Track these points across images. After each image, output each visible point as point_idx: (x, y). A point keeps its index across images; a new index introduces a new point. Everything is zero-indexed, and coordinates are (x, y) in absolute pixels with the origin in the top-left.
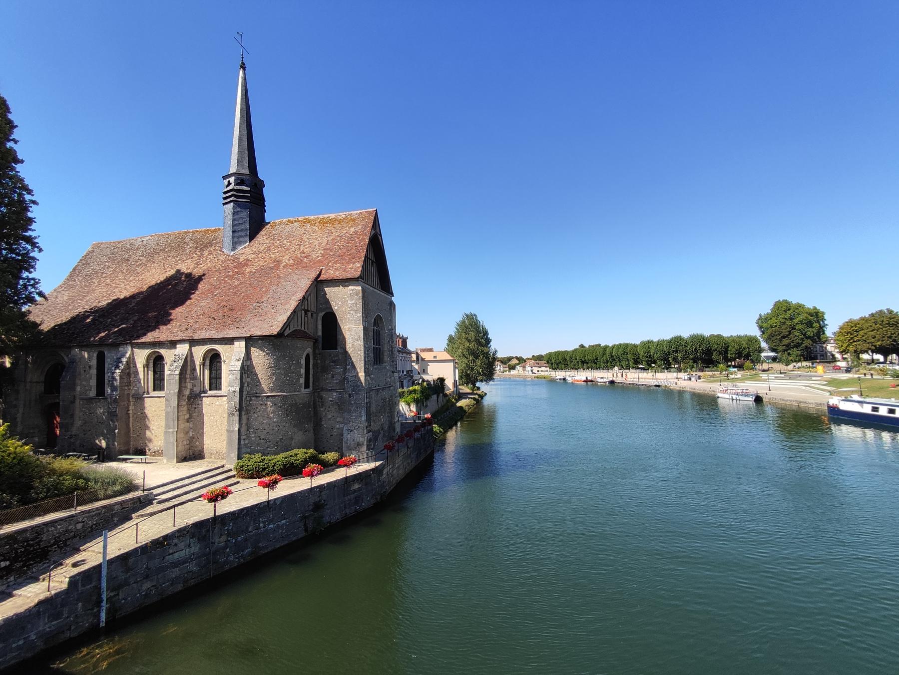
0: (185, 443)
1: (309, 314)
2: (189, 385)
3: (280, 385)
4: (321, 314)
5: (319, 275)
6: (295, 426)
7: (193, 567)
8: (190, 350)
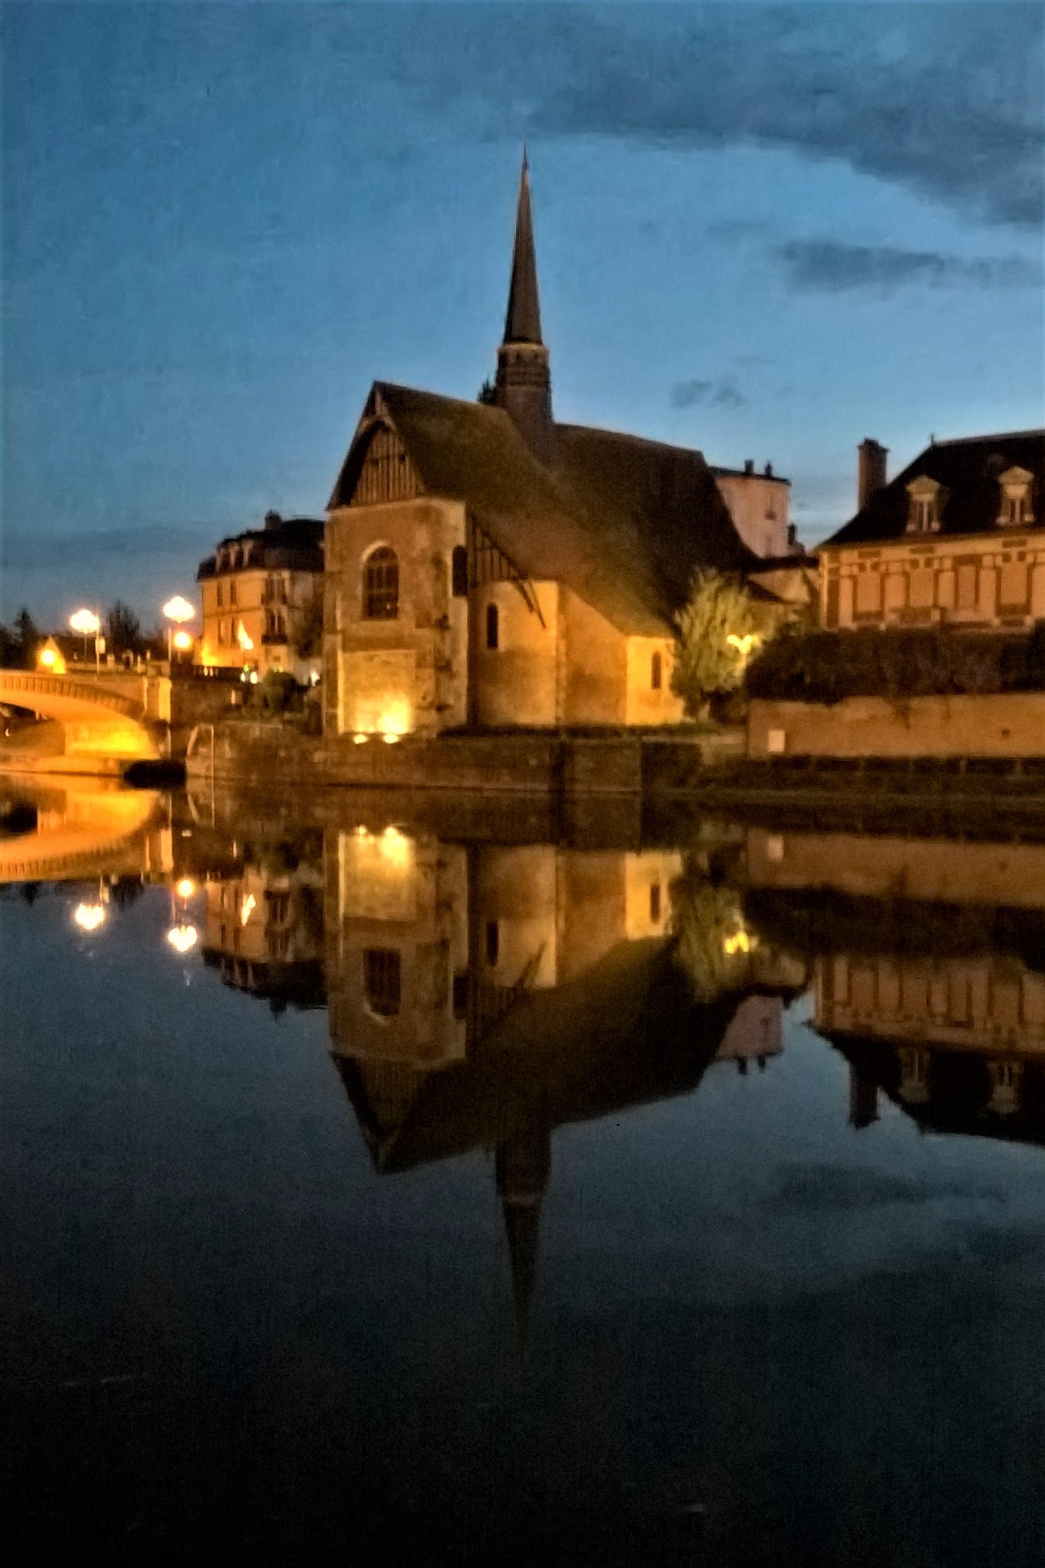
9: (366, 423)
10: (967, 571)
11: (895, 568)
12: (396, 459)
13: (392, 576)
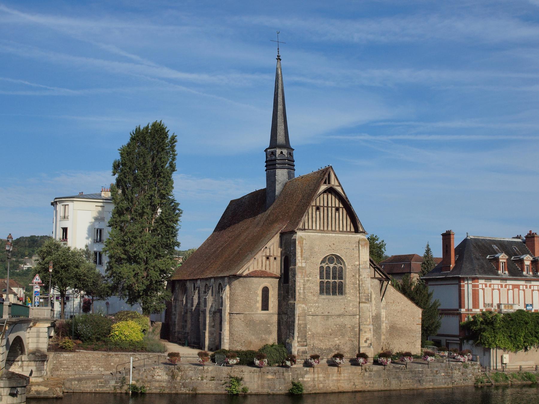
1: (272, 259)
7: (164, 384)
10: (516, 290)
11: (496, 287)
12: (334, 209)
13: (339, 274)
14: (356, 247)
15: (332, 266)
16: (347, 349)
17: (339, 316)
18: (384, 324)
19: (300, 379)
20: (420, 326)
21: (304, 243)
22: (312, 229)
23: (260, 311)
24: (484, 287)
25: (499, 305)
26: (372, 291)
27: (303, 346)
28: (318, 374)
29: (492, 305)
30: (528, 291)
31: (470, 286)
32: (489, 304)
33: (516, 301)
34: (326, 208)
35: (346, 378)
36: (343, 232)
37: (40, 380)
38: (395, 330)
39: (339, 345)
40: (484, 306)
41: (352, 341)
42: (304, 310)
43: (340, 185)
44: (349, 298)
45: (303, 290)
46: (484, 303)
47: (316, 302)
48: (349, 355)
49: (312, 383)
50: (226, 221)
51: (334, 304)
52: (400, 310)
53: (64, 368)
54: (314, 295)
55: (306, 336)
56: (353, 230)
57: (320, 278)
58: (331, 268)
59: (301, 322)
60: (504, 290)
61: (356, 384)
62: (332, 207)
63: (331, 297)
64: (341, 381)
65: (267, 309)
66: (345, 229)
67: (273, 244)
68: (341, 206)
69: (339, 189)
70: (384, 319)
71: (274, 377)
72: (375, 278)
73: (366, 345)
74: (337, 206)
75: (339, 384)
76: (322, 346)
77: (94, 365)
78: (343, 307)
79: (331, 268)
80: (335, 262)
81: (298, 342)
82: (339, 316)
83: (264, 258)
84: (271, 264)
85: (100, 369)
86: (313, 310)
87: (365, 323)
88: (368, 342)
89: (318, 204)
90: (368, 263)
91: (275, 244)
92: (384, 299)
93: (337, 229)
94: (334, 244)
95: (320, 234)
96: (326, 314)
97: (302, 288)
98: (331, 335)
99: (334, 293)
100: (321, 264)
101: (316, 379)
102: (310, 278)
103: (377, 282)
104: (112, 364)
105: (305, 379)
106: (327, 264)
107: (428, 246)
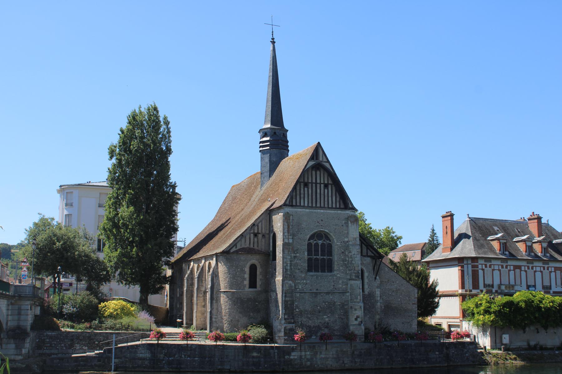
0: (202, 320)
2: (204, 285)
3: (231, 286)
4: (272, 235)
5: (272, 205)
6: (240, 313)
8: (205, 263)
9: (311, 163)
10: (518, 271)
11: (496, 267)
12: (322, 185)
13: (328, 250)
14: (345, 223)
15: (320, 242)
16: (337, 328)
17: (328, 293)
18: (379, 304)
19: (286, 357)
20: (416, 306)
21: (291, 219)
22: (300, 206)
23: (247, 289)
24: (484, 267)
25: (499, 286)
26: (364, 269)
27: (290, 323)
28: (305, 352)
29: (492, 286)
30: (530, 272)
31: (470, 266)
32: (489, 285)
33: (518, 282)
34: (314, 185)
35: (335, 356)
36: (332, 208)
37: (20, 357)
38: (389, 309)
39: (328, 323)
40: (484, 287)
41: (342, 319)
42: (290, 286)
43: (328, 161)
44: (338, 275)
45: (290, 266)
46: (484, 284)
47: (305, 279)
48: (339, 334)
49: (299, 361)
50: (226, 206)
51: (323, 282)
52: (395, 290)
53: (47, 347)
54: (302, 272)
55: (293, 313)
56: (342, 206)
57: (308, 255)
58: (320, 244)
59: (287, 299)
60: (504, 270)
61: (345, 362)
62: (320, 184)
63: (320, 274)
64: (329, 360)
65: (255, 287)
66: (334, 206)
67: (261, 221)
68: (330, 182)
69: (327, 165)
70: (379, 299)
71: (259, 355)
72: (368, 256)
73: (357, 322)
74: (326, 182)
75: (327, 362)
76: (310, 323)
77: (77, 344)
78: (333, 284)
79: (320, 244)
80: (324, 238)
81: (285, 319)
82: (328, 293)
83: (252, 235)
84: (260, 241)
85: (84, 347)
86: (300, 287)
87: (355, 300)
88: (359, 320)
89: (306, 180)
90: (358, 239)
91: (263, 221)
92: (377, 277)
93: (326, 206)
94: (322, 220)
95: (308, 210)
96: (315, 291)
97: (289, 265)
98: (319, 312)
99: (323, 271)
100: (309, 240)
101: (303, 357)
102: (298, 255)
103: (368, 260)
104: (96, 343)
105: (292, 357)
106: (315, 240)
107: (433, 230)
